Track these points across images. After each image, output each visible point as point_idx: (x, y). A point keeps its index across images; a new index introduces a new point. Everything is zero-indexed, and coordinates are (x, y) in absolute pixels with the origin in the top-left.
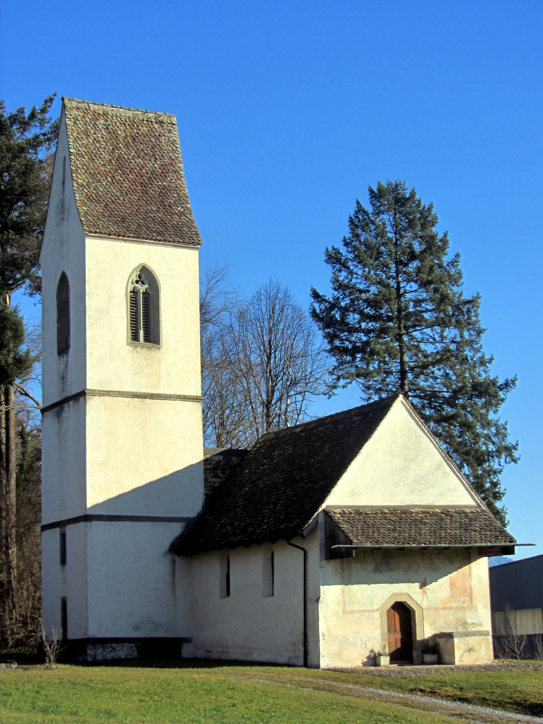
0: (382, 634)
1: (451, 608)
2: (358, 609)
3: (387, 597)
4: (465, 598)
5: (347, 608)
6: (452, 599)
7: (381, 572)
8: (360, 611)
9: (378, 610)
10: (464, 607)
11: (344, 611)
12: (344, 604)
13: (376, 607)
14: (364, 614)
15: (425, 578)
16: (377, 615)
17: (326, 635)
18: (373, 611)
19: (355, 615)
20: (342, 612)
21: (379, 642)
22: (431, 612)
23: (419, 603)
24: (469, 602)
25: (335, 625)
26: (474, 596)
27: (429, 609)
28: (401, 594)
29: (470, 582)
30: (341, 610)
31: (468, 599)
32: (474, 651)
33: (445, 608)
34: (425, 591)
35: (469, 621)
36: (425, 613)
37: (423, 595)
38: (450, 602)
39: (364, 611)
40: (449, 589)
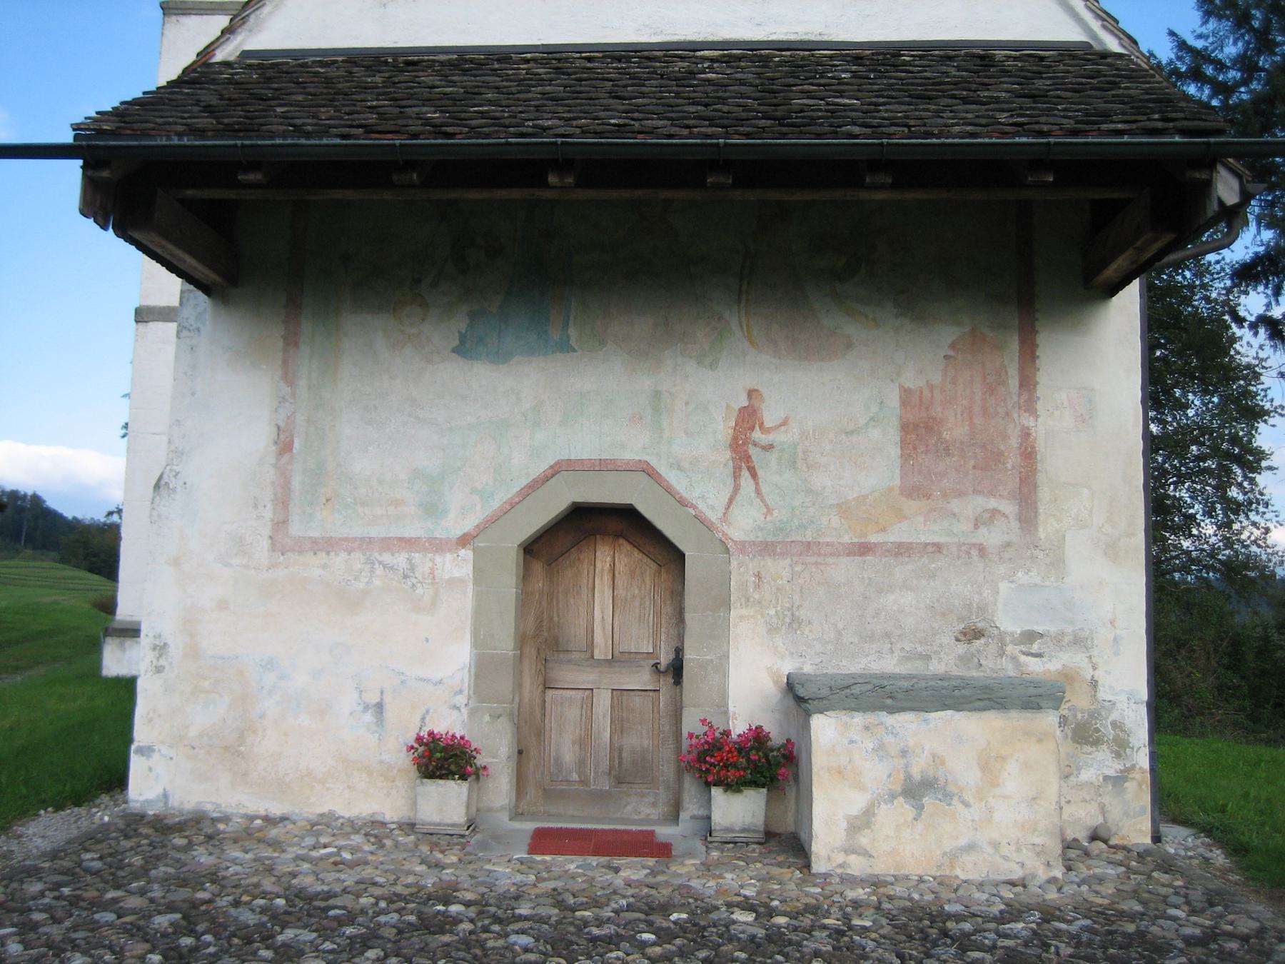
0: (483, 667)
1: (902, 550)
2: (357, 530)
3: (525, 482)
4: (992, 503)
5: (296, 528)
6: (911, 506)
7: (501, 357)
8: (365, 543)
9: (464, 541)
10: (982, 550)
11: (281, 541)
12: (283, 501)
13: (458, 522)
14: (386, 557)
15: (751, 393)
16: (459, 566)
17: (176, 647)
18: (438, 546)
19: (340, 559)
20: (266, 543)
21: (461, 700)
22: (778, 569)
23: (713, 516)
24: (1015, 524)
25: (223, 605)
26: (1044, 493)
27: (767, 548)
28: (603, 467)
29: (1029, 421)
30: (267, 531)
31: (1009, 508)
32: (947, 796)
33: (864, 549)
34: (748, 459)
35: (1009, 623)
36: (741, 571)
37: (736, 476)
38: (901, 516)
39: (389, 544)
40: (895, 452)
